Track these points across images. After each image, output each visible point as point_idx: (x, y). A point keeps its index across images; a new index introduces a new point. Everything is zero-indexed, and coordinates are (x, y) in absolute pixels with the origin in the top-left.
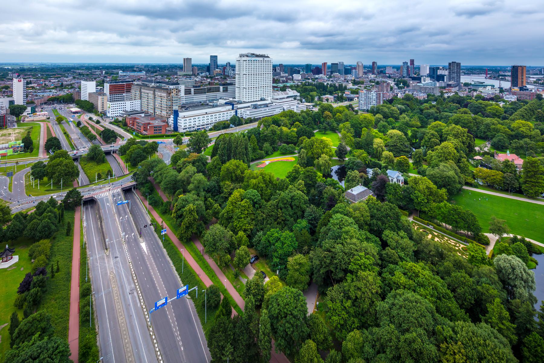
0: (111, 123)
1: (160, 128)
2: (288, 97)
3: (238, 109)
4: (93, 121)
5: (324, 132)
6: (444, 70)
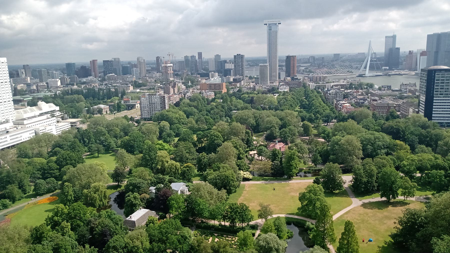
2: (41, 115)
5: (97, 155)
6: (230, 63)
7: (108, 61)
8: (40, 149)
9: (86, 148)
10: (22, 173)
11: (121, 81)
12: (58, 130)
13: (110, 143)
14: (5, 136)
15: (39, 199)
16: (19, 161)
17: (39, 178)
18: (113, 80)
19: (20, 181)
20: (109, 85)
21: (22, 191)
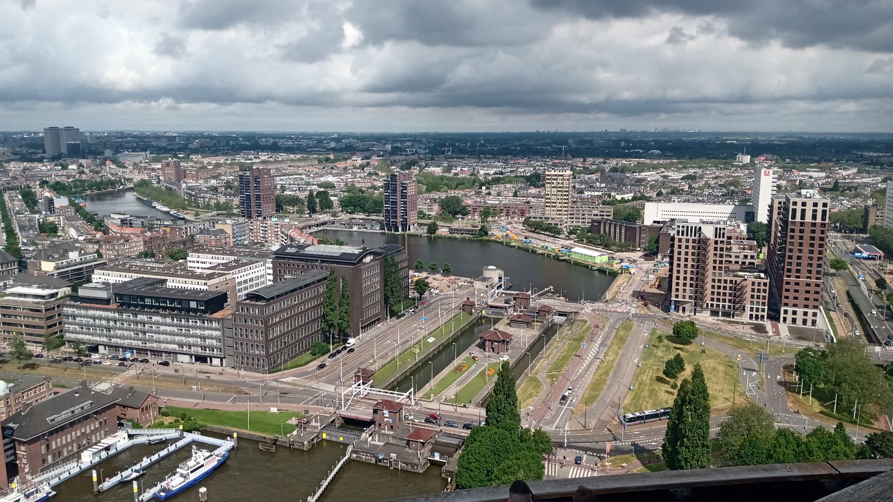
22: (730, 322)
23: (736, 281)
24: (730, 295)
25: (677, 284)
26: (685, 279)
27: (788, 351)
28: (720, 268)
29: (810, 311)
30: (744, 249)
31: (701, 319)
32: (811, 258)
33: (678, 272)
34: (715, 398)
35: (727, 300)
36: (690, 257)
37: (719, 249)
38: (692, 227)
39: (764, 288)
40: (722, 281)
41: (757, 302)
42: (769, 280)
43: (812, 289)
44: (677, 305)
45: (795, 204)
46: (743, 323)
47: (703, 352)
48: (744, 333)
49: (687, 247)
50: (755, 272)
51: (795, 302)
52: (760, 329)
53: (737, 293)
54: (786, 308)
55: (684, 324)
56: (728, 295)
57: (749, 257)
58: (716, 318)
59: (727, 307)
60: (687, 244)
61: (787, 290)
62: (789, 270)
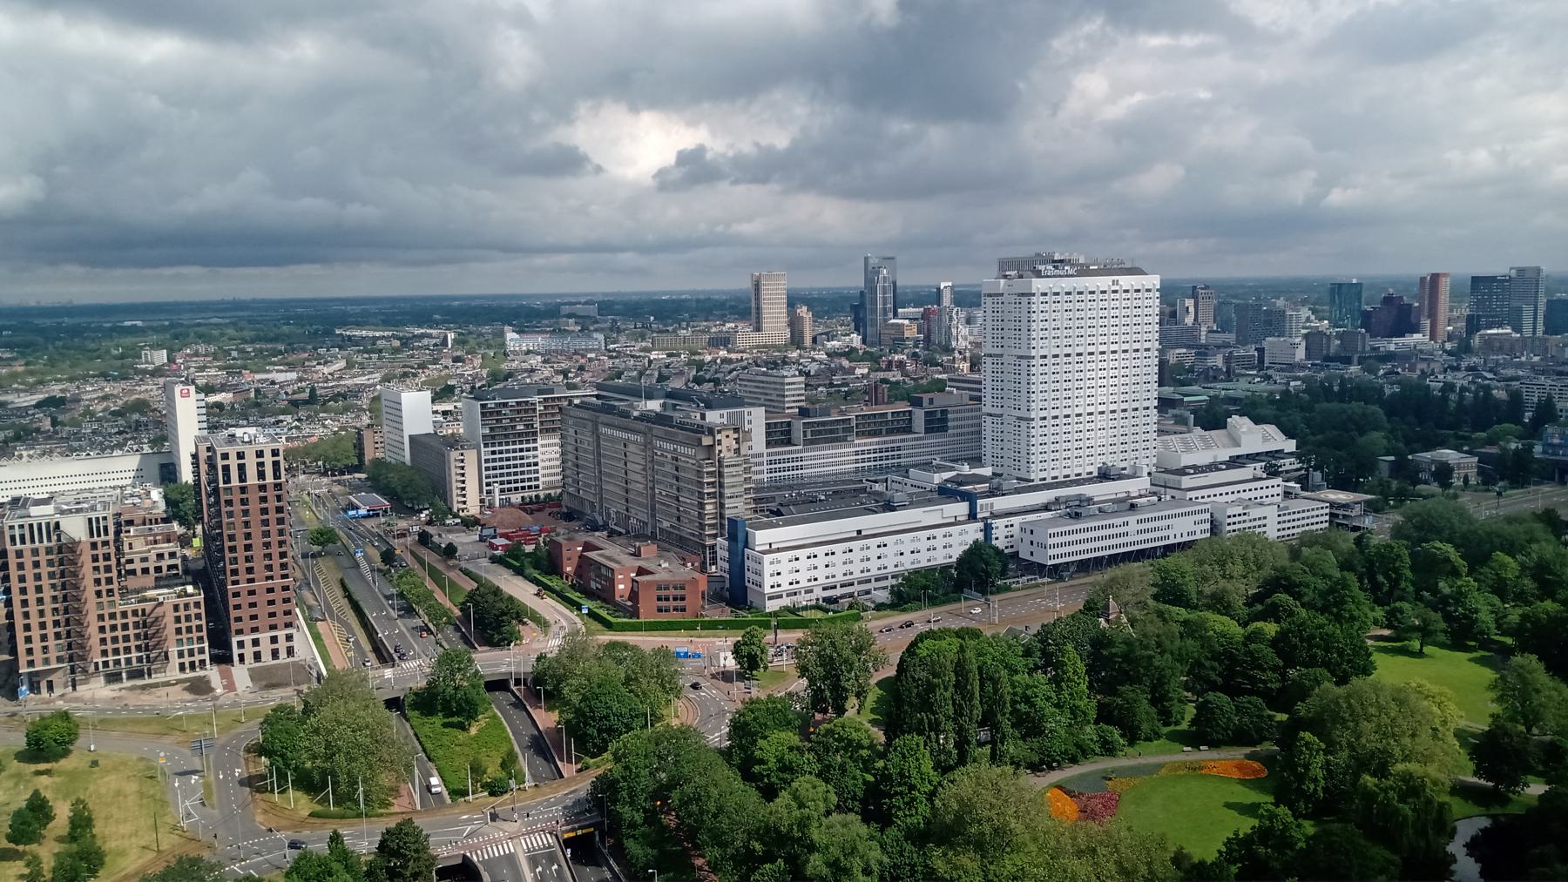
0: (494, 560)
1: (679, 592)
2: (1235, 462)
3: (995, 516)
4: (436, 548)
5: (1416, 645)
7: (1493, 279)
8: (1223, 583)
9: (1379, 613)
10: (1167, 656)
11: (1536, 359)
12: (1284, 522)
13: (1476, 611)
14: (1125, 519)
15: (1205, 754)
16: (1160, 614)
17: (1214, 687)
18: (1500, 350)
19: (1158, 679)
20: (1485, 374)
21: (1159, 713)
22: (144, 688)
23: (143, 610)
24: (137, 637)
25: (28, 640)
26: (43, 626)
27: (250, 715)
28: (110, 593)
29: (281, 634)
30: (156, 542)
31: (88, 695)
32: (267, 545)
33: (26, 615)
34: (122, 853)
35: (133, 649)
36: (45, 582)
37: (101, 558)
38: (40, 525)
39: (197, 611)
40: (118, 616)
41: (188, 639)
42: (203, 596)
43: (278, 596)
44: (35, 679)
45: (225, 456)
46: (167, 684)
47: (95, 763)
48: (171, 702)
49: (36, 565)
50: (177, 585)
51: (254, 623)
52: (200, 687)
53: (148, 632)
54: (240, 638)
55: (48, 721)
56: (132, 638)
57: (166, 556)
58: (117, 686)
59: (134, 660)
60: (36, 559)
61: (237, 607)
62: (235, 572)
